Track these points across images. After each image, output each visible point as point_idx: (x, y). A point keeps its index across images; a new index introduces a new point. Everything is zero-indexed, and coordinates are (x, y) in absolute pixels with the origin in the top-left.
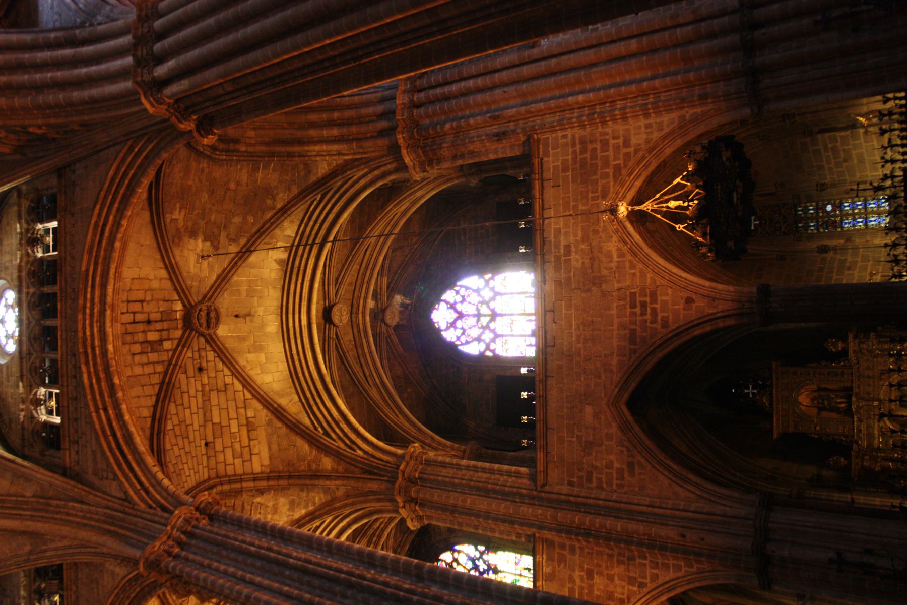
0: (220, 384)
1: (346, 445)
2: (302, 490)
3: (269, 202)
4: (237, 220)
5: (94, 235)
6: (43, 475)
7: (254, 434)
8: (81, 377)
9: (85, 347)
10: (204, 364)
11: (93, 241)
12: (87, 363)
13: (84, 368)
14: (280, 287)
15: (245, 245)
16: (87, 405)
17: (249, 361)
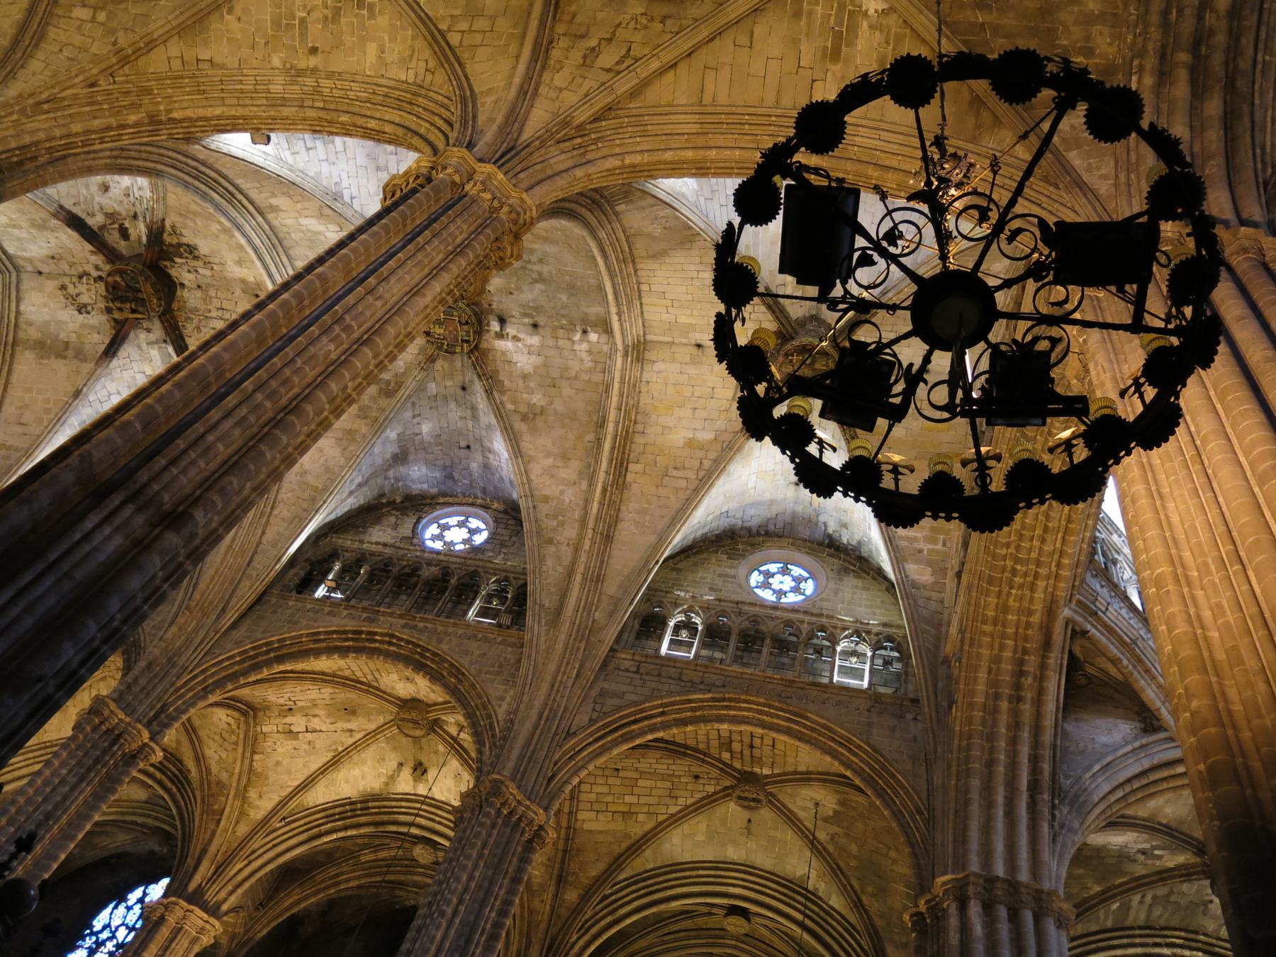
0: (678, 793)
1: (587, 921)
2: (549, 859)
3: (870, 889)
4: (854, 849)
5: (841, 736)
6: (611, 634)
7: (619, 818)
8: (700, 691)
9: (730, 700)
10: (702, 781)
11: (835, 733)
12: (714, 700)
13: (709, 696)
14: (776, 871)
15: (825, 849)
16: (671, 694)
17: (699, 826)
